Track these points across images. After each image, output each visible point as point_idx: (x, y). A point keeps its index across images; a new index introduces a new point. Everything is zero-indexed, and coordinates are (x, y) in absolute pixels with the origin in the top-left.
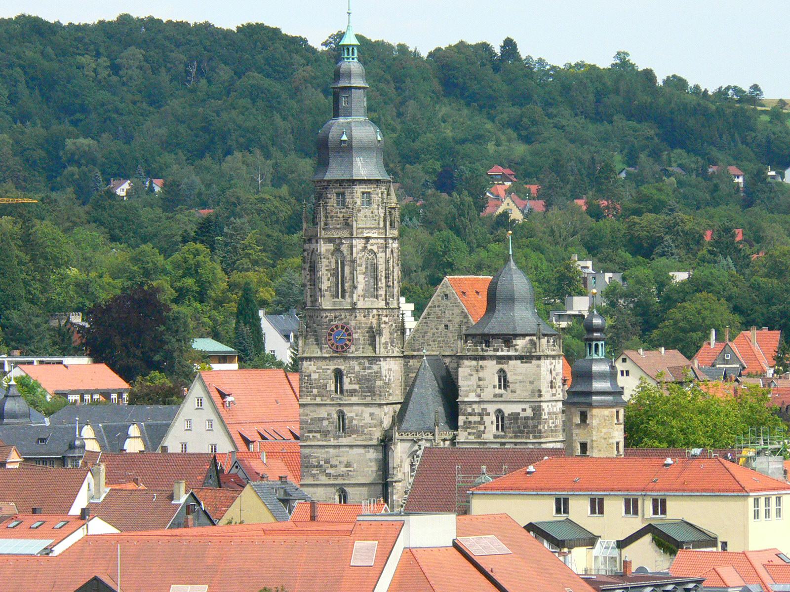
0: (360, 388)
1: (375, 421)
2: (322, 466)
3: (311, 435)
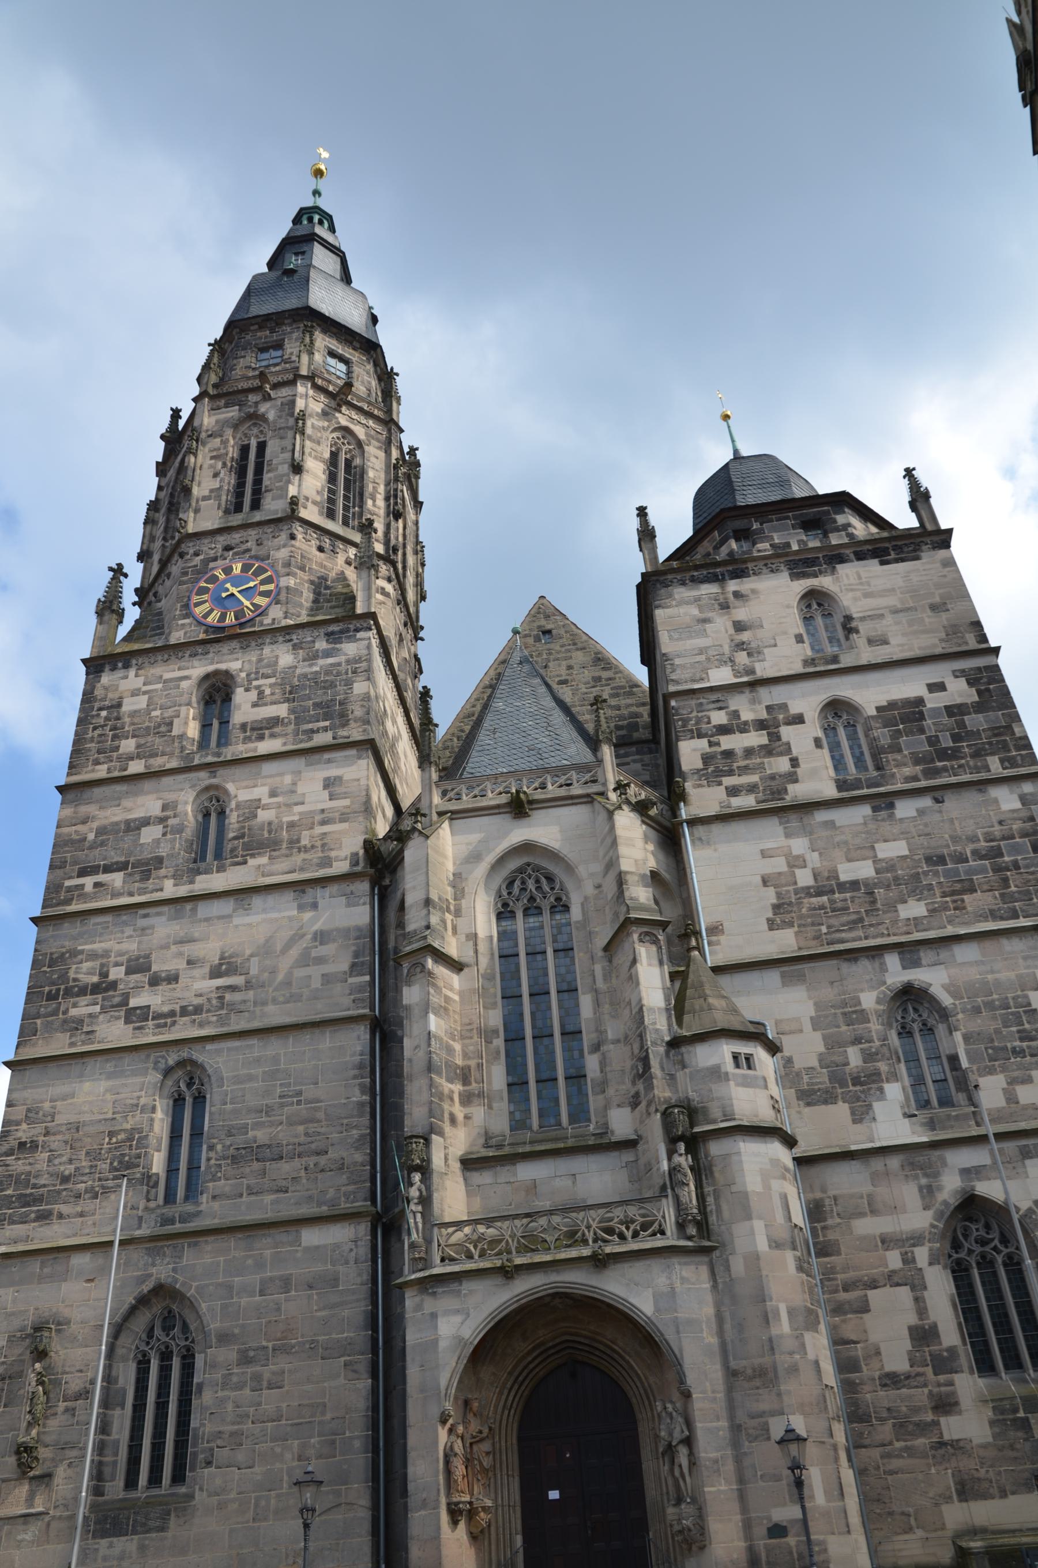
0: (292, 711)
1: (346, 802)
2: (113, 985)
3: (88, 882)
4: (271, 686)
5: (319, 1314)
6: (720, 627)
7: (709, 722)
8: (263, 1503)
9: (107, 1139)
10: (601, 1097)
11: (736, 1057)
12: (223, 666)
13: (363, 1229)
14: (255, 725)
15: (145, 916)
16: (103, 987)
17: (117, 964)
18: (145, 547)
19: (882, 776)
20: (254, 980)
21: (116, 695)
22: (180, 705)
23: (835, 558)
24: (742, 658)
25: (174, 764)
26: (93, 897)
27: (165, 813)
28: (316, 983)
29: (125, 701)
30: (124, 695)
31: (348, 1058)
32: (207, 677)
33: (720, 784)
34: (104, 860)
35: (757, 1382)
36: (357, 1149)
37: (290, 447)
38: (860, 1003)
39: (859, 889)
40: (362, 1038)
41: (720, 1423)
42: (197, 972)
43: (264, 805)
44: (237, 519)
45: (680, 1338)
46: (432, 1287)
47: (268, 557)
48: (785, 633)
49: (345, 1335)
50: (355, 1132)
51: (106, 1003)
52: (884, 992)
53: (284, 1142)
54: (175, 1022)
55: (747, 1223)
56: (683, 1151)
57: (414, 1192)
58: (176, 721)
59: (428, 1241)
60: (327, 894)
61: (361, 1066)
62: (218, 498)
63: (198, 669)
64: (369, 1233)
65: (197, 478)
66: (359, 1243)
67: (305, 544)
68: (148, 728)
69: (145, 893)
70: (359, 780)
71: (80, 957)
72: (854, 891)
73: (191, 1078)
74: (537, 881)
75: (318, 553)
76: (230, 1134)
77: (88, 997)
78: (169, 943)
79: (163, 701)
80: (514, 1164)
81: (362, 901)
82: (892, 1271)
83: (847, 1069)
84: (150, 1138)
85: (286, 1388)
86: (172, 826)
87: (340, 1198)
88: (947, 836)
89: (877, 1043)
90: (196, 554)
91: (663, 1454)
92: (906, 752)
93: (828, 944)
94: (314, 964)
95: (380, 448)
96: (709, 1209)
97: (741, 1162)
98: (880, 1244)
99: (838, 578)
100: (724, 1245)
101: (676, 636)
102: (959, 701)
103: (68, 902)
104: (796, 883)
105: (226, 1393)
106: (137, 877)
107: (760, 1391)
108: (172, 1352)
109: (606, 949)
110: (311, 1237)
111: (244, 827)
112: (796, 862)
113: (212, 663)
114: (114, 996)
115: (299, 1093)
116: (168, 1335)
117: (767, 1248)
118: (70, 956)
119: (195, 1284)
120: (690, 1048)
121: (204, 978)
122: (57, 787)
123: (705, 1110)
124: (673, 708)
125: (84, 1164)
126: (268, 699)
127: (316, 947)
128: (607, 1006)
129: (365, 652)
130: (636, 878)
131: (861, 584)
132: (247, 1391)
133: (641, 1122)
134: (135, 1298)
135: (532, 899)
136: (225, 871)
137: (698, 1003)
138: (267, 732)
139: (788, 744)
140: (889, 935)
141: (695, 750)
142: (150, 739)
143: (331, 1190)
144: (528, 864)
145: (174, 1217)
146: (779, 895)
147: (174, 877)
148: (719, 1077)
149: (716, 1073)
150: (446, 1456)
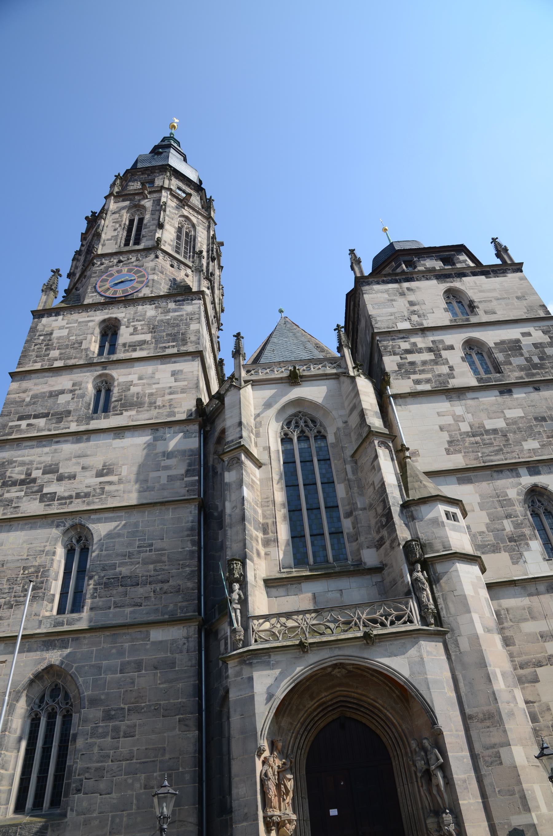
2: (34, 480)
3: (24, 424)
4: (141, 325)
5: (161, 686)
6: (401, 305)
7: (400, 348)
8: (118, 820)
9: (22, 572)
10: (354, 544)
11: (447, 514)
12: (114, 316)
13: (192, 629)
14: (131, 344)
15: (58, 442)
16: (27, 481)
17: (37, 469)
18: (72, 271)
19: (503, 376)
20: (124, 479)
21: (50, 329)
22: (87, 334)
23: (461, 274)
24: (415, 318)
25: (81, 362)
26: (26, 431)
27: (74, 388)
28: (164, 480)
29: (55, 332)
30: (54, 329)
31: (184, 524)
32: (104, 321)
33: (409, 378)
34: (35, 411)
35: (488, 723)
36: (189, 579)
37: (157, 218)
38: (507, 495)
39: (498, 434)
40: (193, 512)
41: (464, 753)
42: (88, 474)
43: (135, 384)
44: (127, 248)
45: (430, 692)
46: (249, 659)
47: (143, 266)
48: (438, 307)
49: (180, 700)
50: (187, 569)
51: (28, 490)
52: (521, 489)
53: (140, 575)
54: (72, 502)
55: (467, 615)
56: (420, 569)
57: (235, 596)
58: (84, 342)
59: (246, 628)
60: (172, 432)
61: (192, 529)
62: (116, 240)
63: (100, 316)
64: (197, 633)
65: (104, 230)
66: (190, 639)
67: (163, 262)
68: (67, 345)
69: (58, 430)
70: (193, 372)
71: (14, 464)
72: (495, 434)
73: (80, 537)
74: (305, 422)
75: (171, 268)
76: (104, 569)
77: (17, 487)
78: (71, 457)
79: (78, 332)
80: (300, 583)
81: (194, 435)
82: (550, 655)
83: (505, 533)
84: (51, 571)
85: (137, 737)
86: (78, 395)
87: (177, 610)
88: (544, 407)
89: (521, 518)
90: (102, 264)
91: (421, 778)
92: (514, 365)
93: (484, 462)
94: (162, 470)
95: (204, 229)
96: (440, 607)
97: (459, 576)
98: (540, 638)
99: (463, 283)
100: (453, 630)
101: (376, 307)
102: (540, 341)
103: (11, 434)
104: (460, 430)
105: (94, 740)
106: (54, 421)
107: (491, 729)
108: (56, 713)
109: (353, 456)
110: (157, 635)
111: (122, 395)
112: (458, 419)
113: (107, 314)
114: (34, 487)
115: (151, 545)
116: (54, 701)
117: (483, 632)
118: (8, 464)
119: (75, 665)
120: (417, 508)
121: (92, 477)
122: (10, 373)
123: (431, 545)
124: (378, 340)
125: (5, 586)
126: (140, 332)
127: (164, 460)
128: (356, 489)
129: (198, 310)
130: (372, 413)
131: (477, 286)
132: (109, 739)
133: (386, 555)
134: (33, 674)
135: (302, 432)
136: (109, 418)
137: (416, 485)
138: (138, 348)
139: (447, 359)
140: (519, 458)
141: (392, 361)
142: (68, 350)
143: (171, 605)
144: (300, 412)
145: (63, 621)
146: (450, 436)
147: (77, 421)
148: (438, 524)
149: (436, 522)
150: (261, 780)
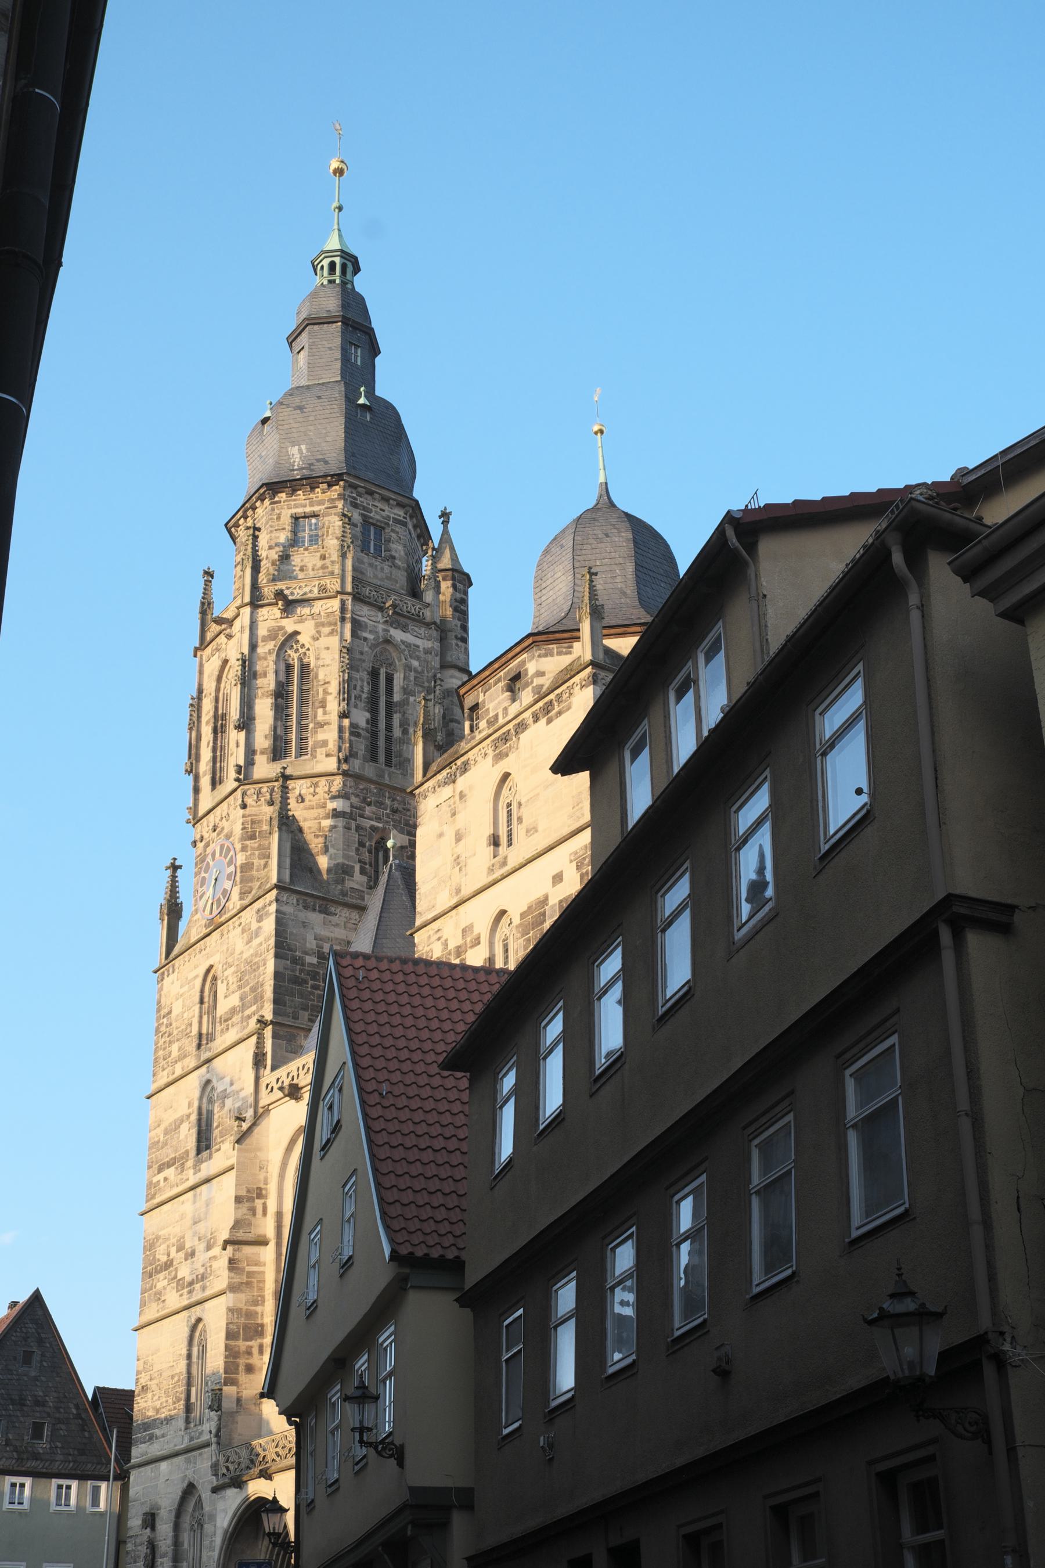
126: (231, 990)
